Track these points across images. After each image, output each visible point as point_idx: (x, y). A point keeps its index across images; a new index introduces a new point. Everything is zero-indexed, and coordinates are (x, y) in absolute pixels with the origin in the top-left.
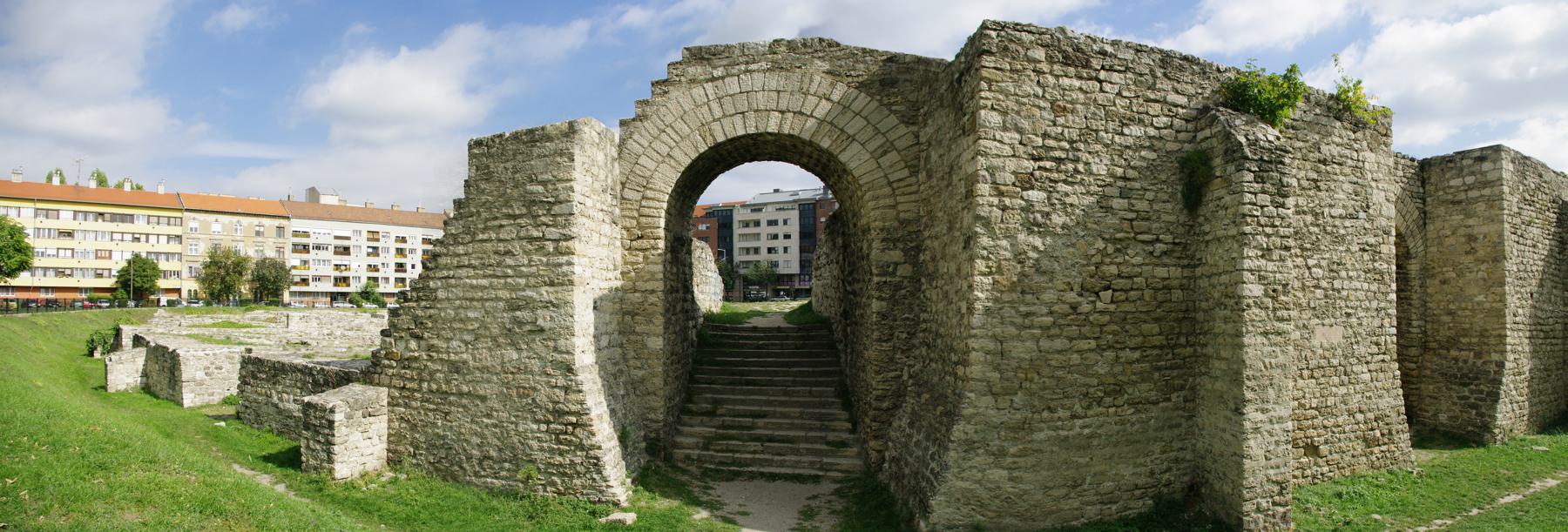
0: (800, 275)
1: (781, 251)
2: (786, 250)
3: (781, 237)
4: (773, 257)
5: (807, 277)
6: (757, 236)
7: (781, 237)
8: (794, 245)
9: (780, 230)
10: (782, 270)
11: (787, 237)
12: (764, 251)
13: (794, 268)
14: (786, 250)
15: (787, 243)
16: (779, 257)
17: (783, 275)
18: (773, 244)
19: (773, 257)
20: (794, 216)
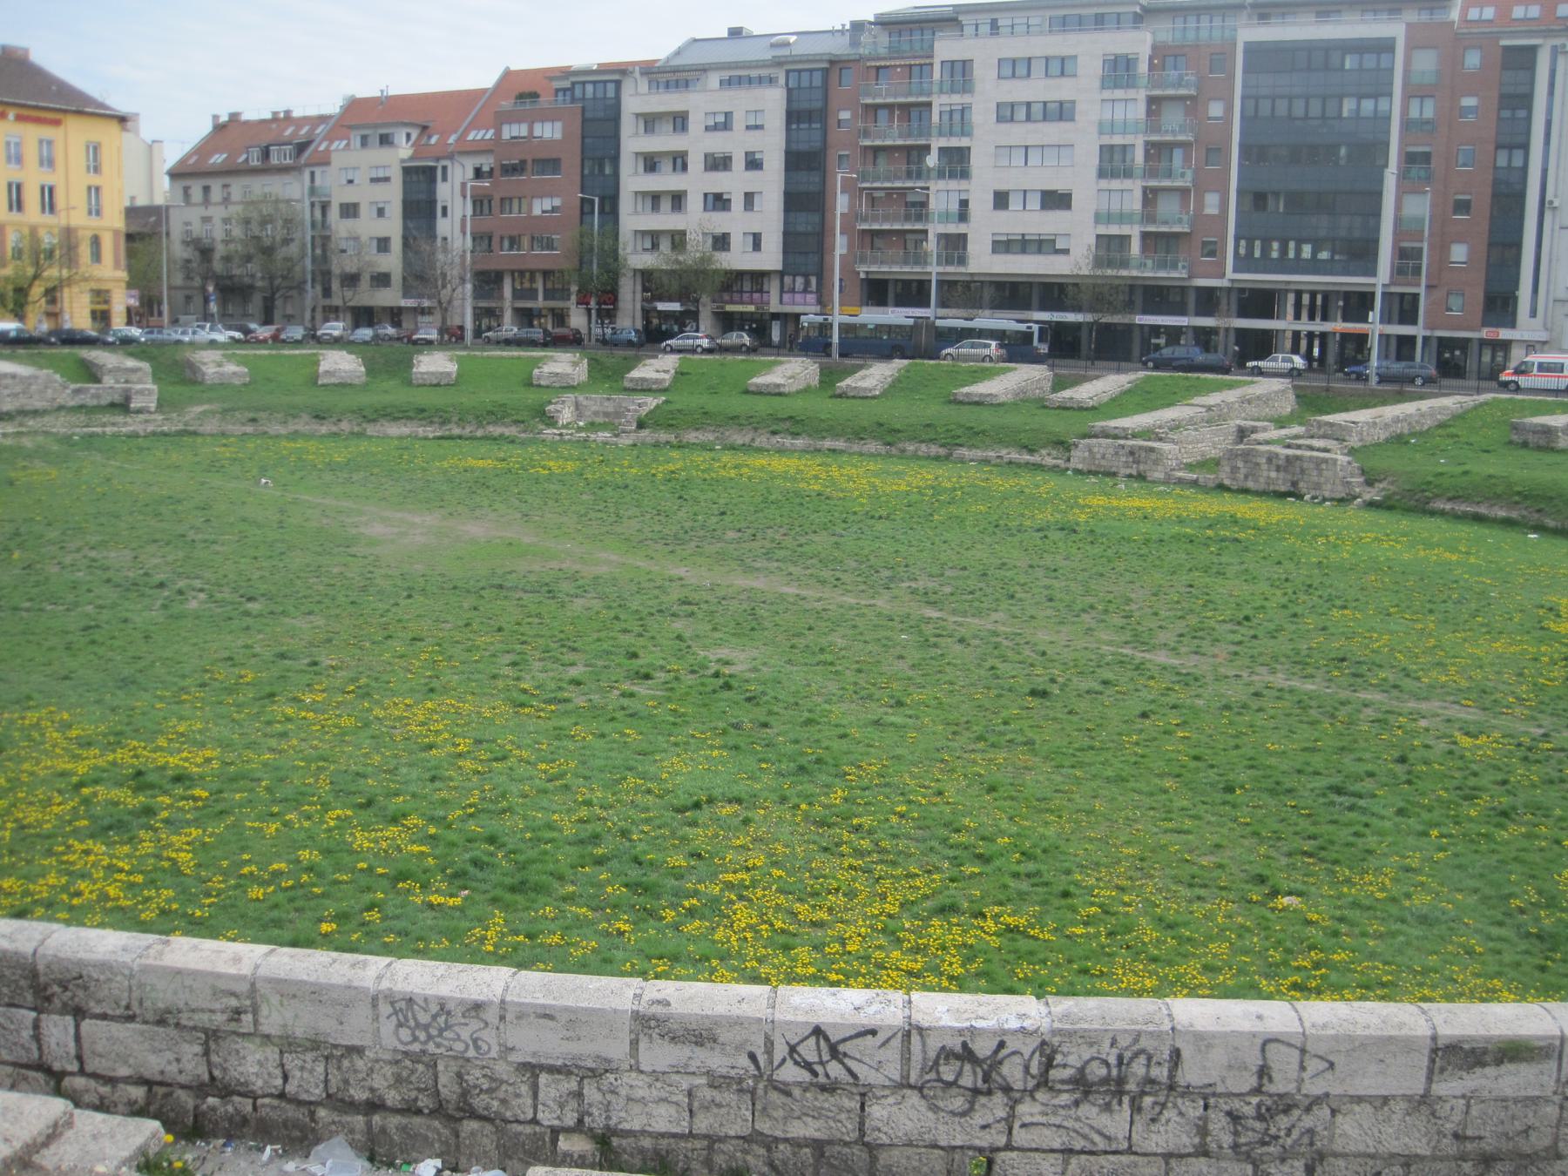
0: (781, 274)
1: (737, 203)
2: (749, 198)
3: (739, 162)
4: (720, 222)
5: (800, 281)
6: (679, 161)
7: (739, 162)
8: (771, 184)
9: (735, 144)
10: (739, 258)
11: (753, 164)
12: (694, 203)
13: (770, 258)
14: (749, 198)
15: (751, 181)
16: (734, 222)
17: (740, 274)
18: (720, 182)
19: (720, 222)
20: (773, 102)
